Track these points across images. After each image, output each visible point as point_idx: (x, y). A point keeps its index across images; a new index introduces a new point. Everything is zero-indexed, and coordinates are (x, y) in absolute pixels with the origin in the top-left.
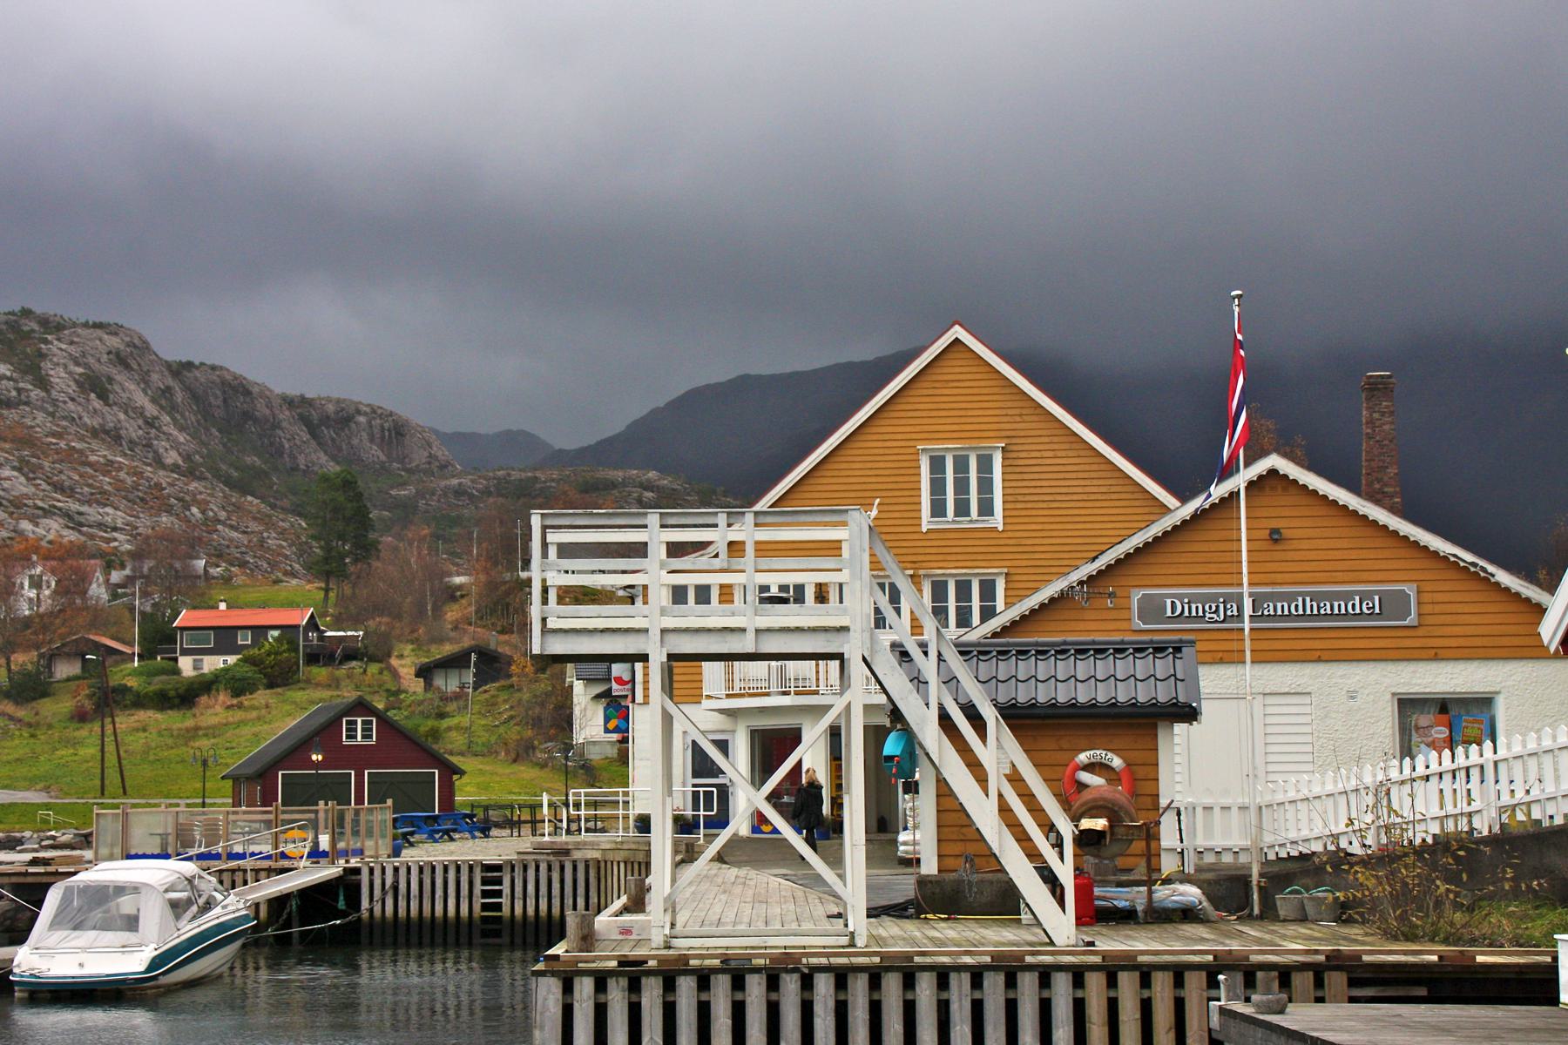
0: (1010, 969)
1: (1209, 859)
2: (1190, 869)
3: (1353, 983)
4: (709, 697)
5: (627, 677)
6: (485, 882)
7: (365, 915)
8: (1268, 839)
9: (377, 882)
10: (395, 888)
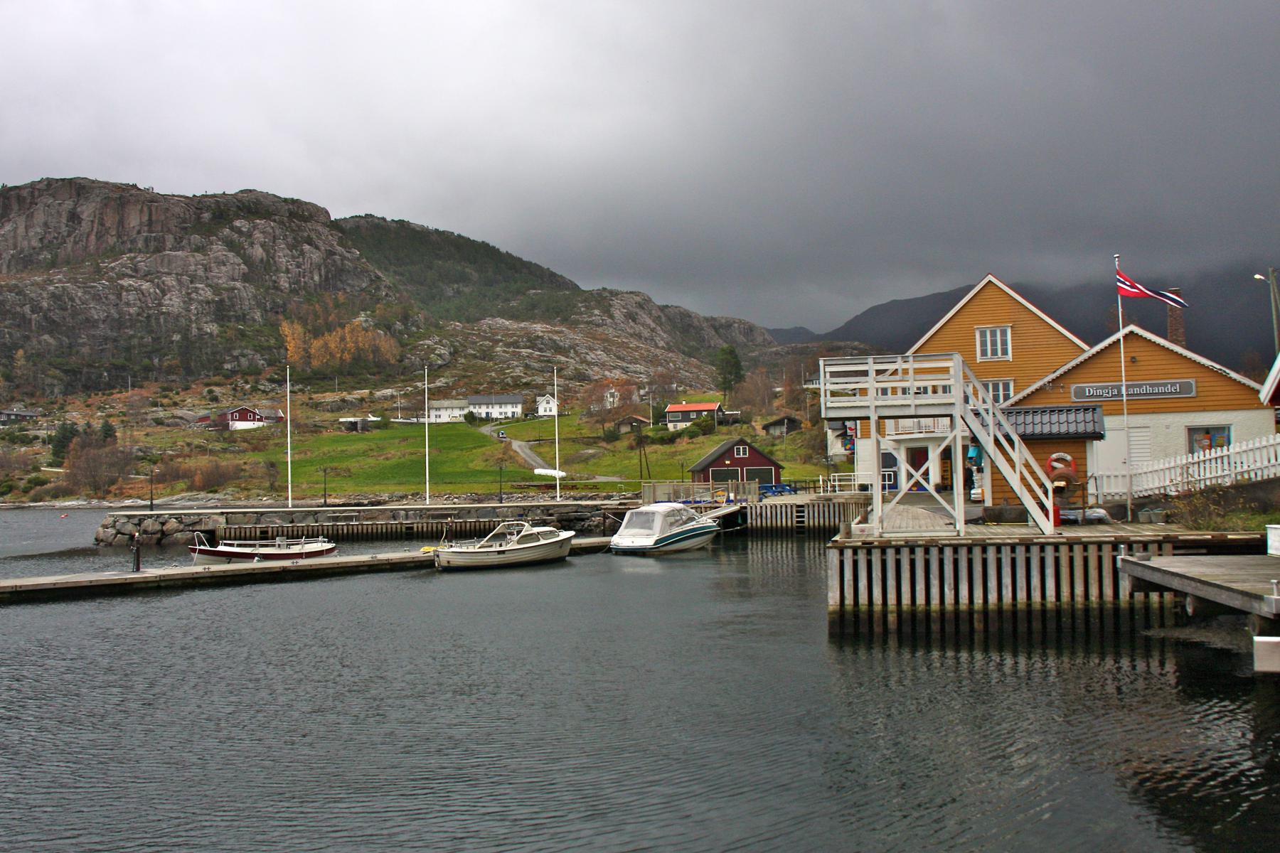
0: (1027, 545)
1: (1109, 498)
2: (1100, 502)
3: (1175, 548)
8: (1135, 488)
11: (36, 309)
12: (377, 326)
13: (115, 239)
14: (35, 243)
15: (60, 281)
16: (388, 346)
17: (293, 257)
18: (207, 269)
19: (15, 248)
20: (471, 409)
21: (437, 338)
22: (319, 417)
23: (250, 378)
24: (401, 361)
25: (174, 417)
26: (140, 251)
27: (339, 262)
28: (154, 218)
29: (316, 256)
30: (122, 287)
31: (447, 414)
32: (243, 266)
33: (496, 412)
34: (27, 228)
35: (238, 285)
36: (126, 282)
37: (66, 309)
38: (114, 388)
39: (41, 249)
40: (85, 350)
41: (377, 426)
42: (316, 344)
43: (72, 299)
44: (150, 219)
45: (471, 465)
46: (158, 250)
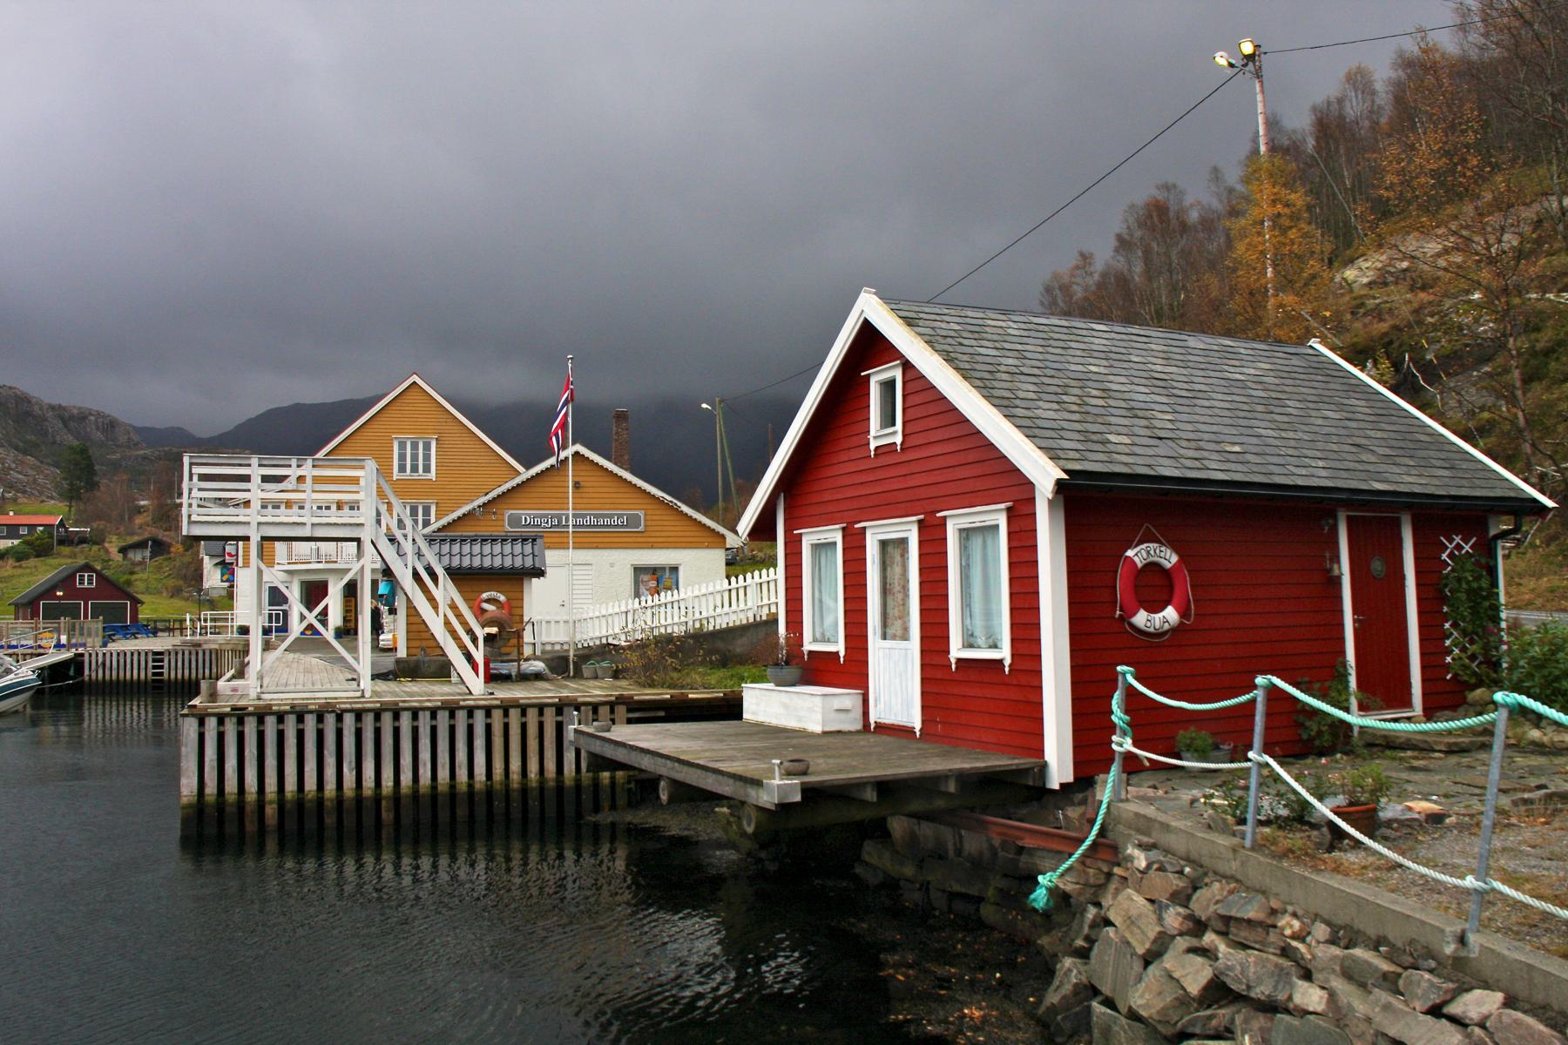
0: (452, 709)
1: (548, 648)
2: (538, 653)
3: (629, 711)
8: (578, 637)
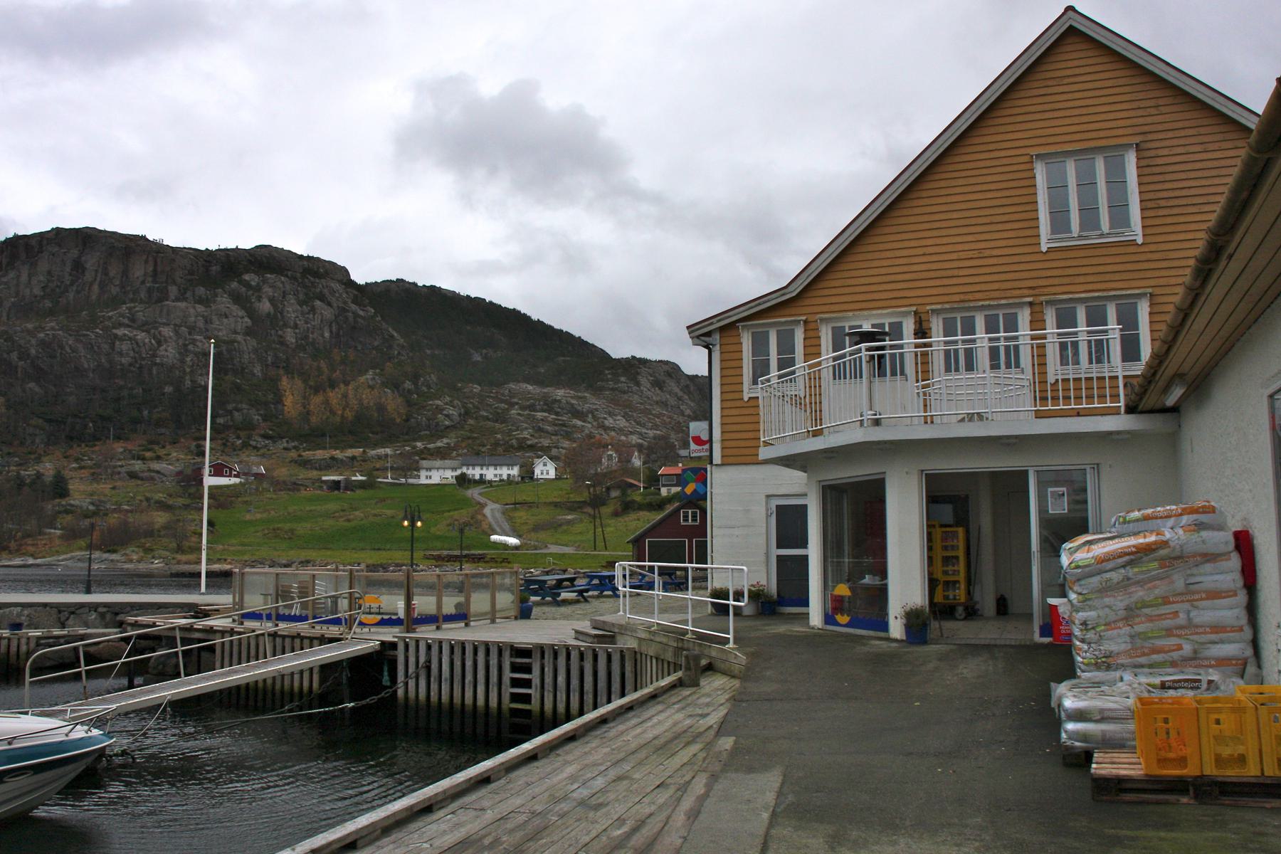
4: (766, 444)
5: (705, 437)
6: (515, 668)
7: (400, 692)
9: (412, 660)
10: (428, 668)
11: (24, 355)
12: (384, 384)
13: (118, 289)
14: (37, 291)
15: (53, 329)
16: (393, 403)
17: (303, 314)
18: (207, 321)
19: (17, 294)
20: (464, 470)
21: (448, 399)
22: (304, 474)
23: (242, 434)
24: (407, 420)
25: (150, 470)
26: (141, 302)
27: (351, 319)
28: (159, 269)
29: (328, 313)
30: (116, 336)
31: (436, 475)
32: (246, 319)
33: (490, 474)
34: (30, 276)
35: (239, 338)
36: (120, 332)
37: (55, 357)
38: (99, 439)
39: (43, 297)
40: (72, 399)
41: (362, 485)
42: (317, 400)
43: (62, 347)
44: (155, 270)
45: (433, 530)
46: (160, 300)
